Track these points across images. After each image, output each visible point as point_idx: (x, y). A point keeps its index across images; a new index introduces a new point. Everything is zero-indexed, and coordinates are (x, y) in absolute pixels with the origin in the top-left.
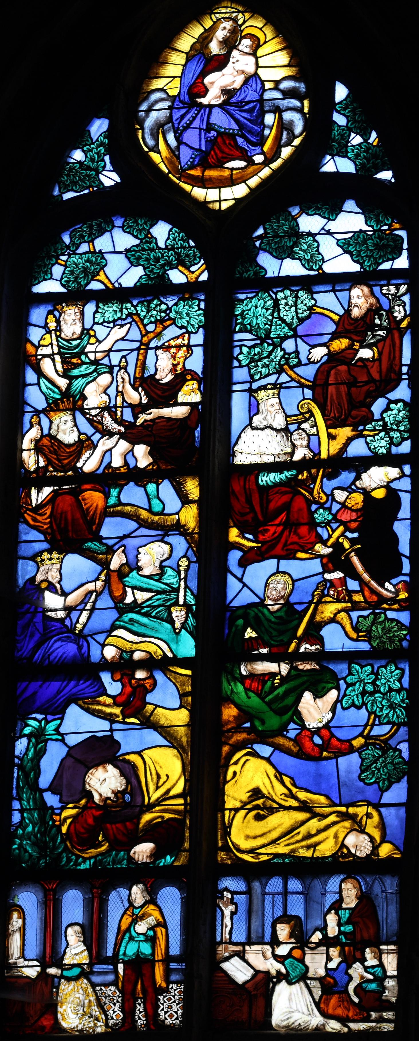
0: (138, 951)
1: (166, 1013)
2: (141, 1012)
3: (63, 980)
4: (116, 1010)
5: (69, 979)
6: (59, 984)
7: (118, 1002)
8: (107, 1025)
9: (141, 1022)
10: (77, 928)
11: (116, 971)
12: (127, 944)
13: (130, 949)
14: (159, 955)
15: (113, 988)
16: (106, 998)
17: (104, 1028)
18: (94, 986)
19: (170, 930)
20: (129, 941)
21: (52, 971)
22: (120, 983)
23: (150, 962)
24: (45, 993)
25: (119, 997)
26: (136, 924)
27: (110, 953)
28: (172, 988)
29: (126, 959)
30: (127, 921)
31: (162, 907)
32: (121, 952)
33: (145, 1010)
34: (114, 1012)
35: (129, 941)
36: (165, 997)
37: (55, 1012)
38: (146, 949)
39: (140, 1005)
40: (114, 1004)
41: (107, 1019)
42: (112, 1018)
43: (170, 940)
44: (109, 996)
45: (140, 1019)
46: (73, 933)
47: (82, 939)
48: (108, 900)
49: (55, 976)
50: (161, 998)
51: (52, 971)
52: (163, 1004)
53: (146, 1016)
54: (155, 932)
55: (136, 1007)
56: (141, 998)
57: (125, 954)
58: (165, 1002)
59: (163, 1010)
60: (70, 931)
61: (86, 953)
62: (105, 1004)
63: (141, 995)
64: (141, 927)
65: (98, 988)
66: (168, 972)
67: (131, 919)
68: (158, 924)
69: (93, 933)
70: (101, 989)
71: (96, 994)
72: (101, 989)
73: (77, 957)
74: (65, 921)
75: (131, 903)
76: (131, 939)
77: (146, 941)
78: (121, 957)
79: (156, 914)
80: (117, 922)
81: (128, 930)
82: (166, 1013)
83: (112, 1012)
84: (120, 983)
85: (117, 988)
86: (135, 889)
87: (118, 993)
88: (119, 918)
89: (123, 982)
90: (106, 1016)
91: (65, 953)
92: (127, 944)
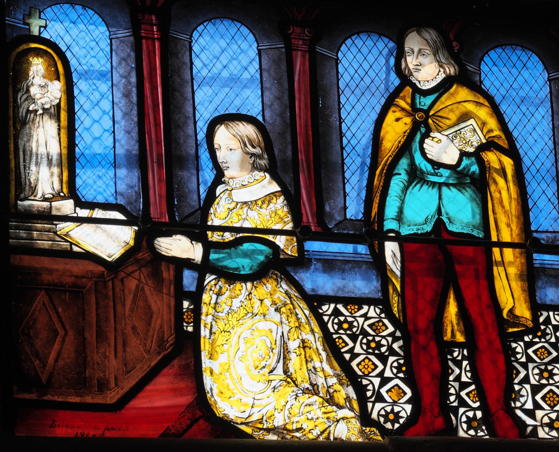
0: (439, 211)
1: (536, 389)
2: (464, 386)
3: (209, 278)
4: (388, 374)
5: (232, 277)
6: (201, 288)
7: (392, 352)
8: (365, 418)
9: (467, 417)
10: (248, 130)
11: (378, 262)
12: (405, 189)
13: (414, 208)
14: (506, 230)
15: (373, 312)
16: (354, 337)
17: (356, 424)
18: (314, 301)
19: (526, 161)
20: (410, 183)
21: (177, 246)
22: (395, 300)
23: (481, 246)
24: (159, 312)
25: (395, 339)
26: (426, 135)
27: (354, 209)
28: (547, 321)
29: (405, 231)
30: (395, 129)
31: (498, 99)
32: (391, 211)
33: (476, 378)
34: (385, 381)
35: (410, 183)
36: (528, 345)
37: (196, 373)
38: (461, 210)
39: (459, 364)
40: (383, 359)
41: (362, 400)
42: (380, 398)
43: (529, 190)
44: (365, 333)
45: (463, 403)
46: (235, 144)
47: (263, 163)
48: (337, 61)
49: (188, 263)
50: (519, 347)
51: (177, 246)
52: (525, 366)
53: (481, 394)
54: (481, 162)
55: (447, 372)
56: (461, 346)
57: (400, 218)
58: (530, 359)
59: (526, 380)
60: (224, 136)
61: (280, 203)
62: (354, 356)
63: (460, 338)
64: (443, 148)
65: (327, 309)
66: (532, 277)
67: (408, 120)
68: (490, 145)
69: (300, 151)
70: (336, 313)
71: (323, 326)
72: (336, 313)
73: (253, 214)
74: (204, 114)
75: (405, 79)
76: (415, 176)
77: (460, 185)
78: (390, 225)
79: (484, 113)
80: (370, 126)
81: (404, 149)
82: (536, 389)
83: (377, 381)
84: (395, 300)
85: (387, 310)
86: (413, 42)
87: (391, 329)
88: (374, 116)
89: (402, 296)
90: (360, 390)
91: (211, 197)
92: (405, 189)
